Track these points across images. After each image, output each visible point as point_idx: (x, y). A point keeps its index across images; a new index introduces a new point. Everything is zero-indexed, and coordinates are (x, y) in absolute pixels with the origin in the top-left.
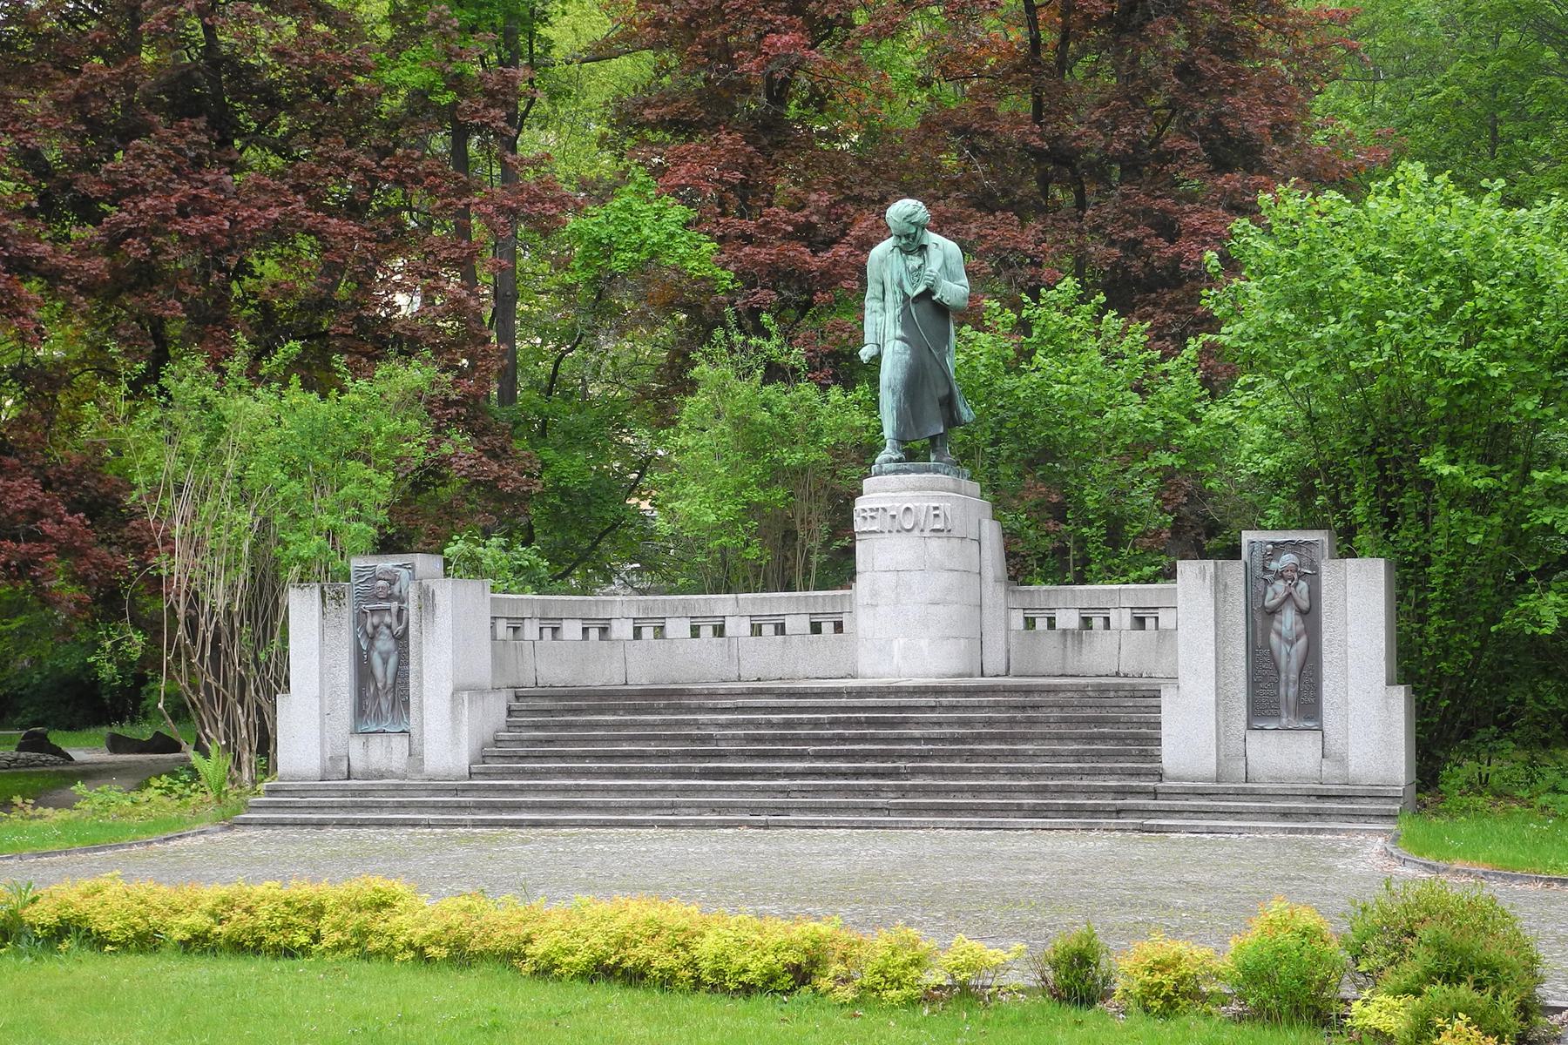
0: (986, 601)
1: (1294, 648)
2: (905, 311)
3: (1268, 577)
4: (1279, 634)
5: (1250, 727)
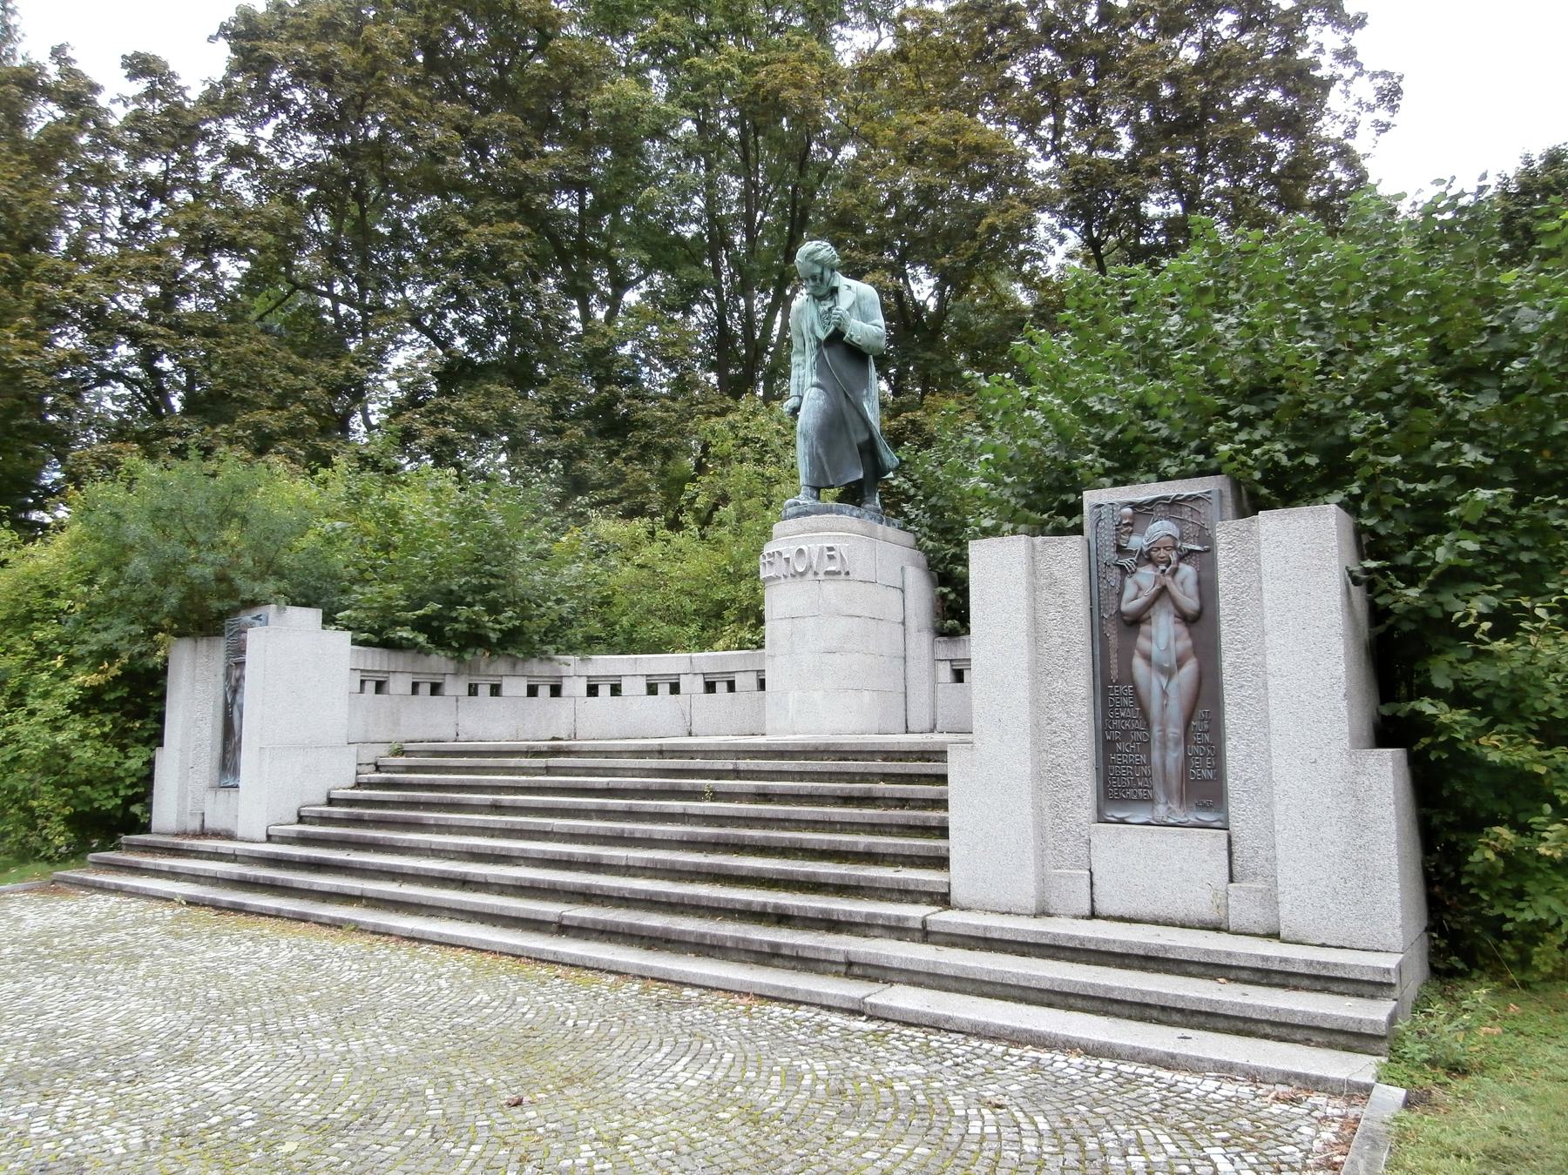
0: (910, 653)
1: (1175, 681)
2: (820, 356)
3: (1125, 561)
4: (1147, 658)
5: (1102, 820)
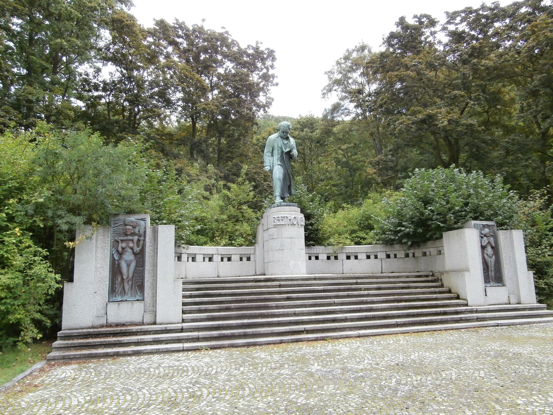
2: (282, 157)
4: (487, 255)
